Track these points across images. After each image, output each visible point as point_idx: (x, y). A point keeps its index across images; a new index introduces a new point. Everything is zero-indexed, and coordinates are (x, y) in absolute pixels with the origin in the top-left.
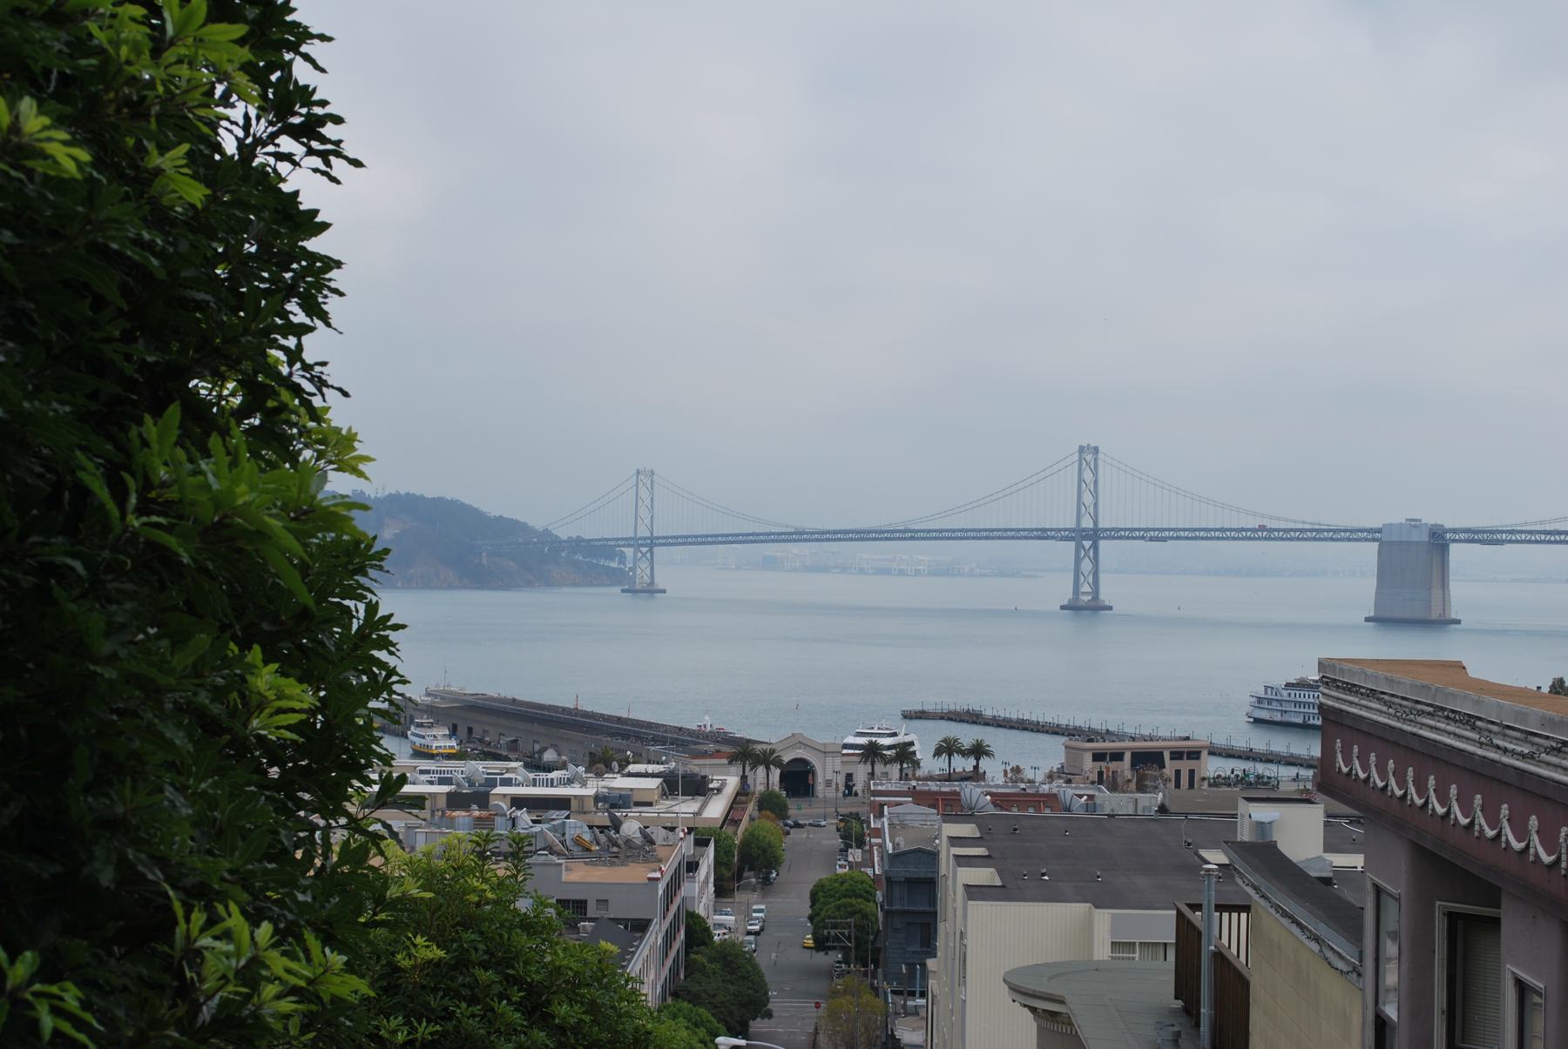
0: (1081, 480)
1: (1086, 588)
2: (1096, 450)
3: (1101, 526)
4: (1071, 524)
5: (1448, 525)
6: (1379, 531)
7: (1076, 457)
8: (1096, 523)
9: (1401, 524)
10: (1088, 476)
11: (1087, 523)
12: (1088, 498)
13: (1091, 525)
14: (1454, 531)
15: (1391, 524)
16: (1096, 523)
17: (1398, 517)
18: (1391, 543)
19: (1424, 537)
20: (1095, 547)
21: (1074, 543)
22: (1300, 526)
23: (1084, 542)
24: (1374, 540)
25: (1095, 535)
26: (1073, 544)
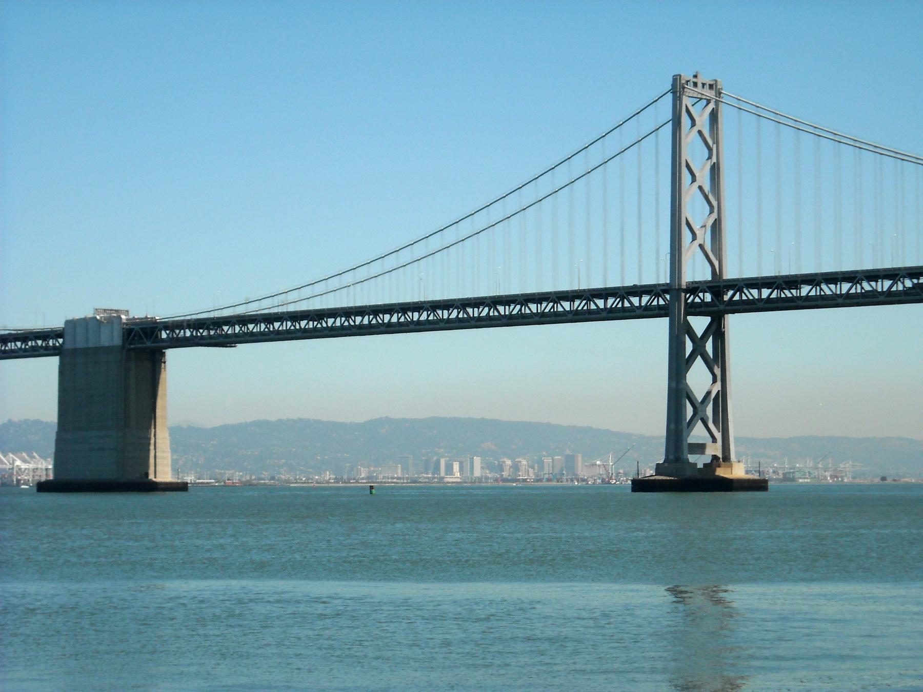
3: (731, 273)
7: (666, 107)
13: (704, 274)
20: (717, 331)
21: (668, 318)
23: (690, 318)
26: (662, 325)
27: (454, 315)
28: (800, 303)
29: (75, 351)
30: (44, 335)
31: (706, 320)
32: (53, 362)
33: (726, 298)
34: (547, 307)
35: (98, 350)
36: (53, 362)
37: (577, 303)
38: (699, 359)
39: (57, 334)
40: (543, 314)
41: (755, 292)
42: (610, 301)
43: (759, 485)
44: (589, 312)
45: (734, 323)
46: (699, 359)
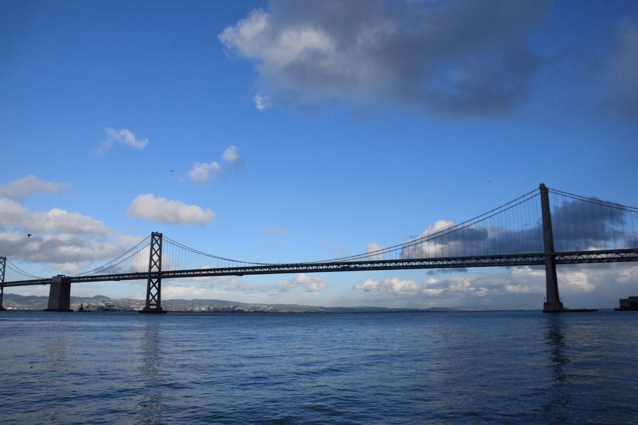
0: (152, 248)
1: (153, 302)
2: (160, 236)
3: (163, 270)
4: (147, 271)
8: (159, 268)
10: (156, 247)
11: (155, 269)
12: (156, 258)
13: (157, 270)
20: (159, 282)
22: (251, 265)
23: (152, 279)
26: (146, 281)
27: (220, 272)
29: (55, 283)
30: (48, 279)
31: (157, 280)
32: (50, 285)
35: (57, 283)
36: (50, 285)
38: (154, 287)
39: (51, 279)
42: (250, 270)
45: (162, 280)
46: (154, 287)
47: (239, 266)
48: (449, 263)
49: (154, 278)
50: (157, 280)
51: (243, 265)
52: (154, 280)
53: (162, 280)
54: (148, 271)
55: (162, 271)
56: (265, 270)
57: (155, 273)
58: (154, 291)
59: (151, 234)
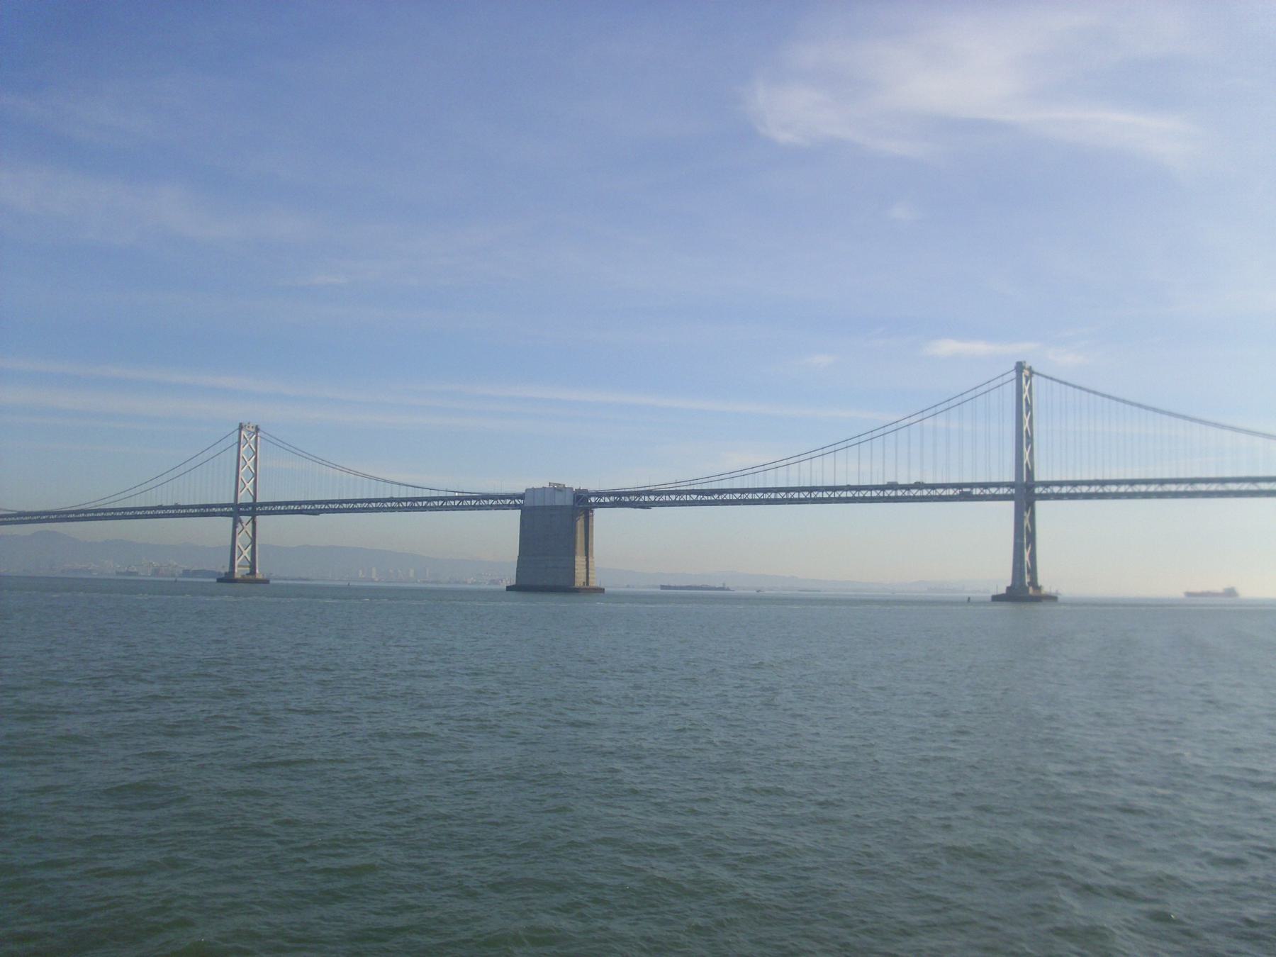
2: (257, 429)
5: (592, 486)
6: (522, 497)
9: (544, 488)
11: (245, 497)
13: (250, 500)
14: (599, 494)
15: (533, 488)
16: (255, 498)
17: (540, 483)
18: (534, 508)
19: (569, 501)
22: (443, 494)
24: (516, 507)
25: (254, 509)
26: (230, 520)
28: (304, 512)
31: (250, 517)
33: (257, 509)
34: (365, 505)
37: (379, 504)
40: (364, 508)
41: (469, 502)
43: (266, 582)
44: (246, 511)
45: (259, 518)
47: (420, 496)
48: (933, 493)
49: (246, 514)
50: (250, 517)
51: (426, 494)
52: (245, 519)
53: (259, 518)
54: (232, 502)
55: (257, 501)
56: (436, 503)
57: (247, 505)
58: (243, 539)
59: (237, 427)
